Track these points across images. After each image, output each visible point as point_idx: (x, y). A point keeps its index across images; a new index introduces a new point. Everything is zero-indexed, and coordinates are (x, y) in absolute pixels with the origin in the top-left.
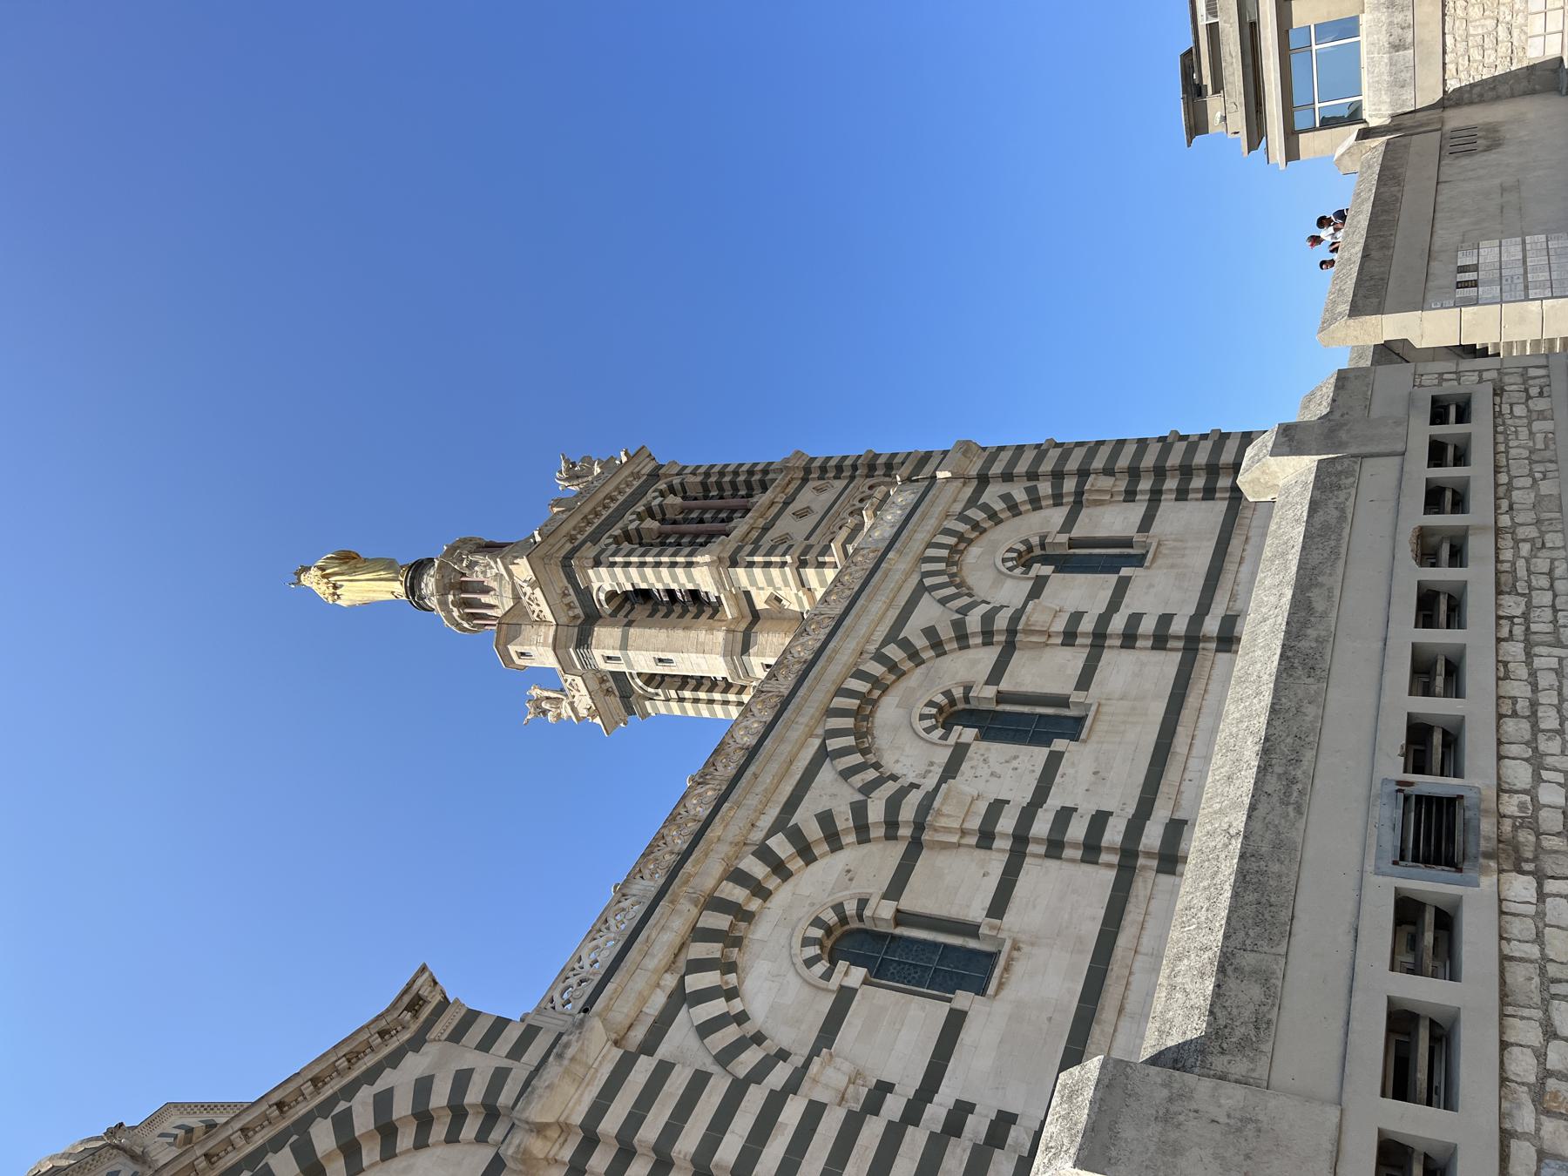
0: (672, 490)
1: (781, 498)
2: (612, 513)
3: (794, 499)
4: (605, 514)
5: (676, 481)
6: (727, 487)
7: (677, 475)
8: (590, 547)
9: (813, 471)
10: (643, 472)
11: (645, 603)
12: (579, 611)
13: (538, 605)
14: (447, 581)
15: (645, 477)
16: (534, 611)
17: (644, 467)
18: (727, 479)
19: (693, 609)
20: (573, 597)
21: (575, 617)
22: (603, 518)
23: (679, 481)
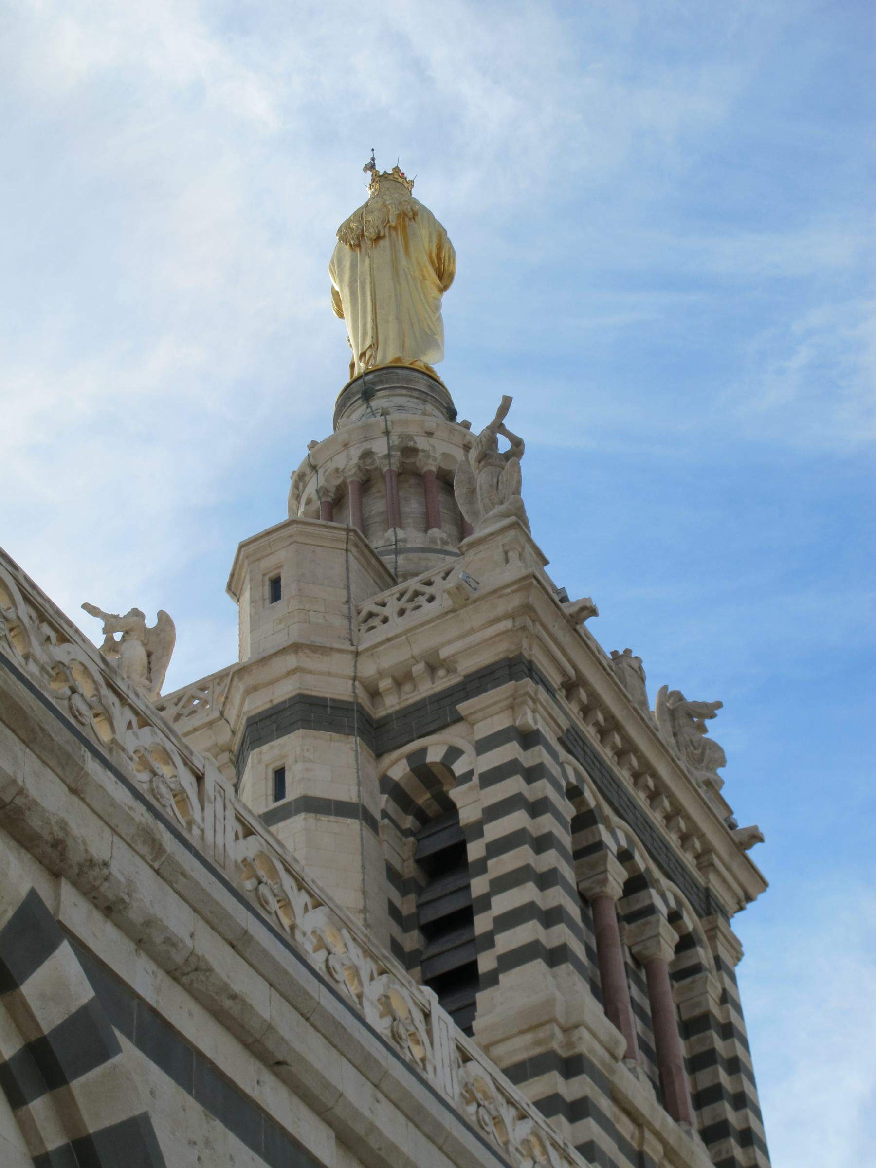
0: (686, 943)
2: (626, 794)
4: (624, 776)
5: (703, 955)
6: (705, 1079)
8: (559, 727)
10: (712, 877)
11: (418, 862)
12: (391, 704)
13: (402, 612)
15: (701, 881)
16: (384, 605)
17: (724, 881)
18: (724, 1078)
20: (426, 689)
21: (375, 694)
22: (616, 769)
23: (704, 961)
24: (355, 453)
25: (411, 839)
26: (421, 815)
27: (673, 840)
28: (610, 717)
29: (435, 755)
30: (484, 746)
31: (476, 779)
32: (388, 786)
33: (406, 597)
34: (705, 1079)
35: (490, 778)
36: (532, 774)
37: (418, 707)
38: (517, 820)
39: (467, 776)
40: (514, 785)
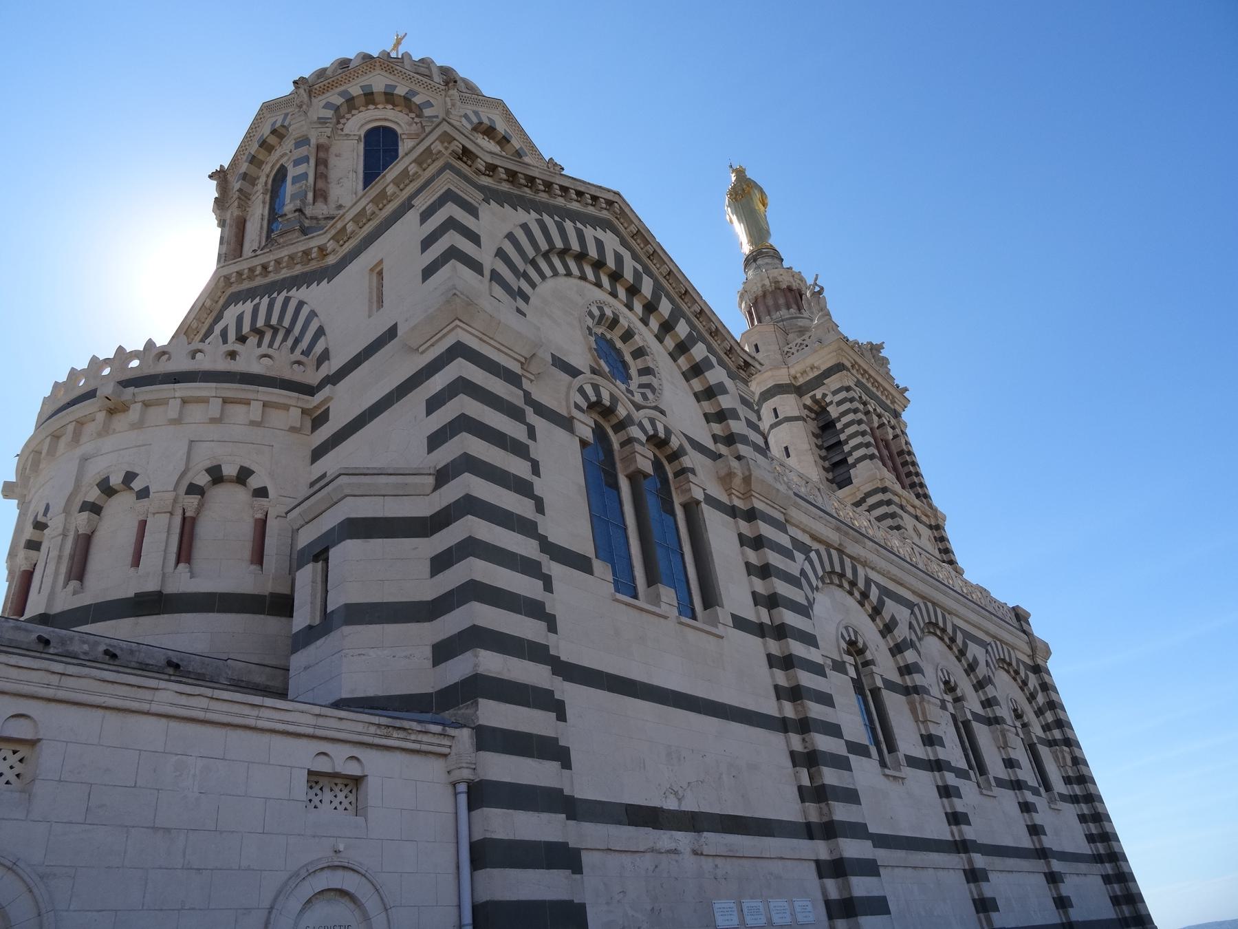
1: (919, 513)
3: (920, 523)
6: (906, 470)
7: (902, 431)
9: (939, 531)
10: (895, 405)
11: (819, 428)
12: (801, 381)
13: (798, 351)
14: (780, 279)
15: (893, 407)
17: (899, 405)
19: (827, 464)
20: (812, 375)
21: (795, 378)
24: (759, 285)
25: (816, 422)
26: (815, 412)
27: (884, 398)
28: (864, 370)
29: (819, 396)
30: (835, 393)
31: (834, 403)
32: (805, 406)
33: (798, 346)
34: (906, 470)
35: (839, 403)
36: (852, 400)
37: (810, 380)
38: (850, 417)
39: (831, 402)
40: (847, 406)
